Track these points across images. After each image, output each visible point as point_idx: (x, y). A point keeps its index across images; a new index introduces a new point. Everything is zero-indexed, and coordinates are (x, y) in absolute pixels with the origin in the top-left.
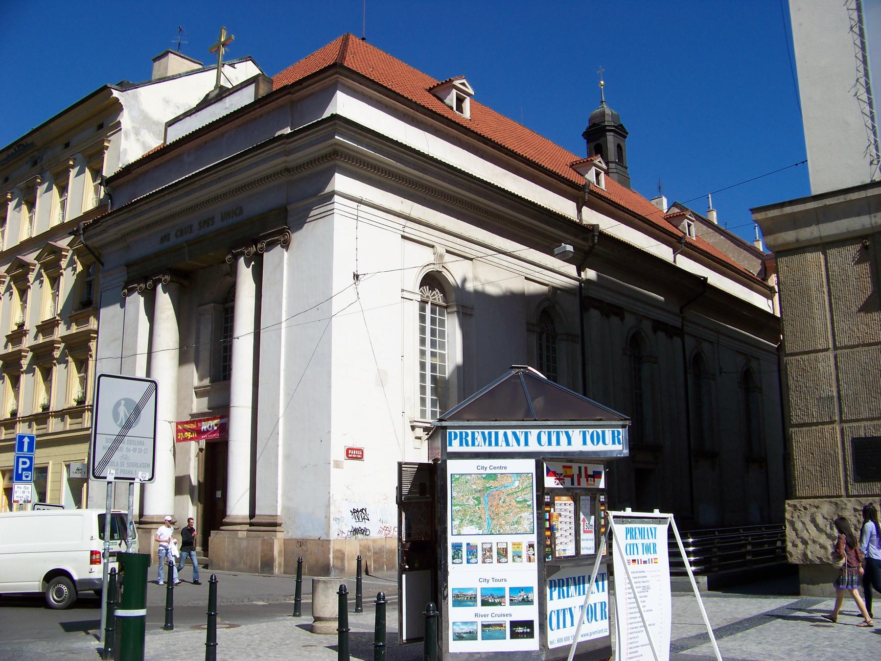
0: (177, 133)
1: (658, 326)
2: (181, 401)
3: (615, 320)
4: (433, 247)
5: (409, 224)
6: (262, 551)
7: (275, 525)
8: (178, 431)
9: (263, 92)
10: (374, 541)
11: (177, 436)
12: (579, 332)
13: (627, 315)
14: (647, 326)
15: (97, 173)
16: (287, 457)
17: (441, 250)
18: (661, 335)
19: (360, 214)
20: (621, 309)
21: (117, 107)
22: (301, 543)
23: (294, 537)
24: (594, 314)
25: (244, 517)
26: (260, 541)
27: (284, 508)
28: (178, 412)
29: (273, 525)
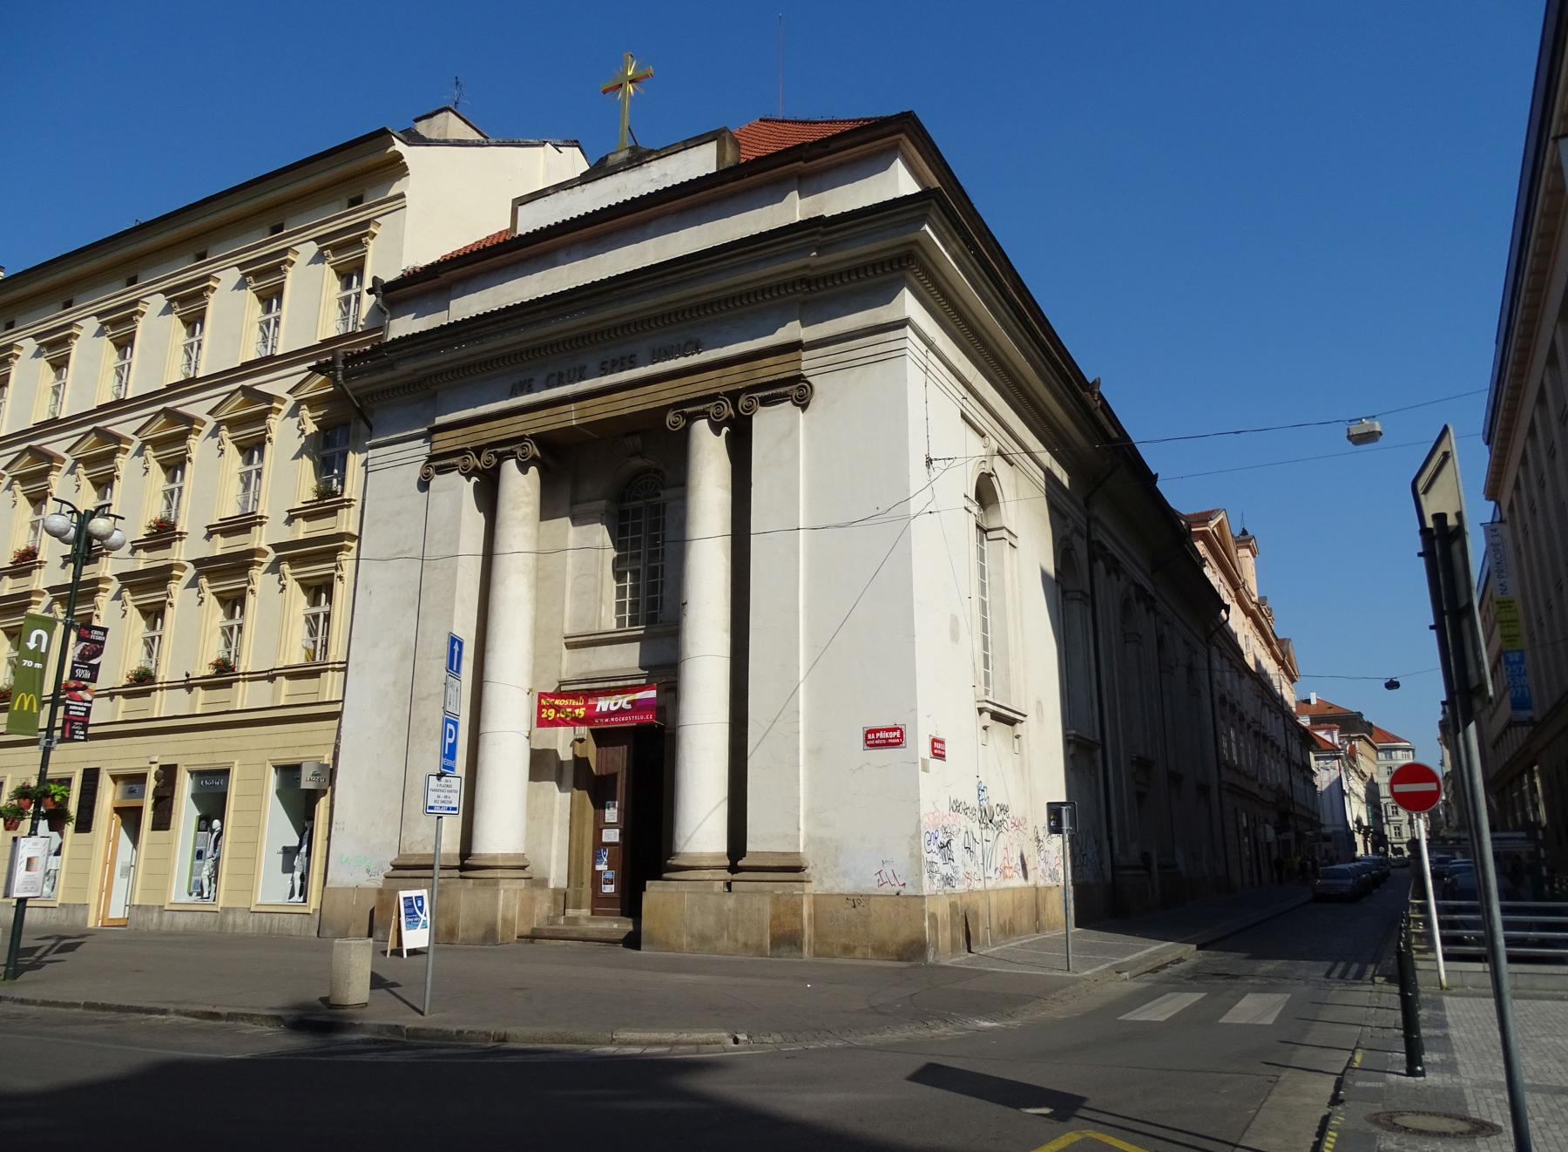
0: (534, 219)
1: (1141, 592)
2: (539, 657)
3: (1114, 577)
4: (983, 436)
5: (970, 397)
6: (775, 917)
7: (798, 869)
8: (540, 707)
9: (730, 159)
10: (961, 896)
11: (540, 713)
12: (1088, 591)
13: (1122, 577)
14: (1132, 590)
15: (349, 273)
16: (816, 752)
17: (995, 445)
18: (1142, 605)
19: (930, 367)
20: (1118, 562)
21: (397, 167)
22: (855, 900)
23: (837, 891)
24: (1101, 564)
25: (716, 856)
26: (768, 899)
27: (810, 840)
28: (535, 678)
29: (793, 869)
